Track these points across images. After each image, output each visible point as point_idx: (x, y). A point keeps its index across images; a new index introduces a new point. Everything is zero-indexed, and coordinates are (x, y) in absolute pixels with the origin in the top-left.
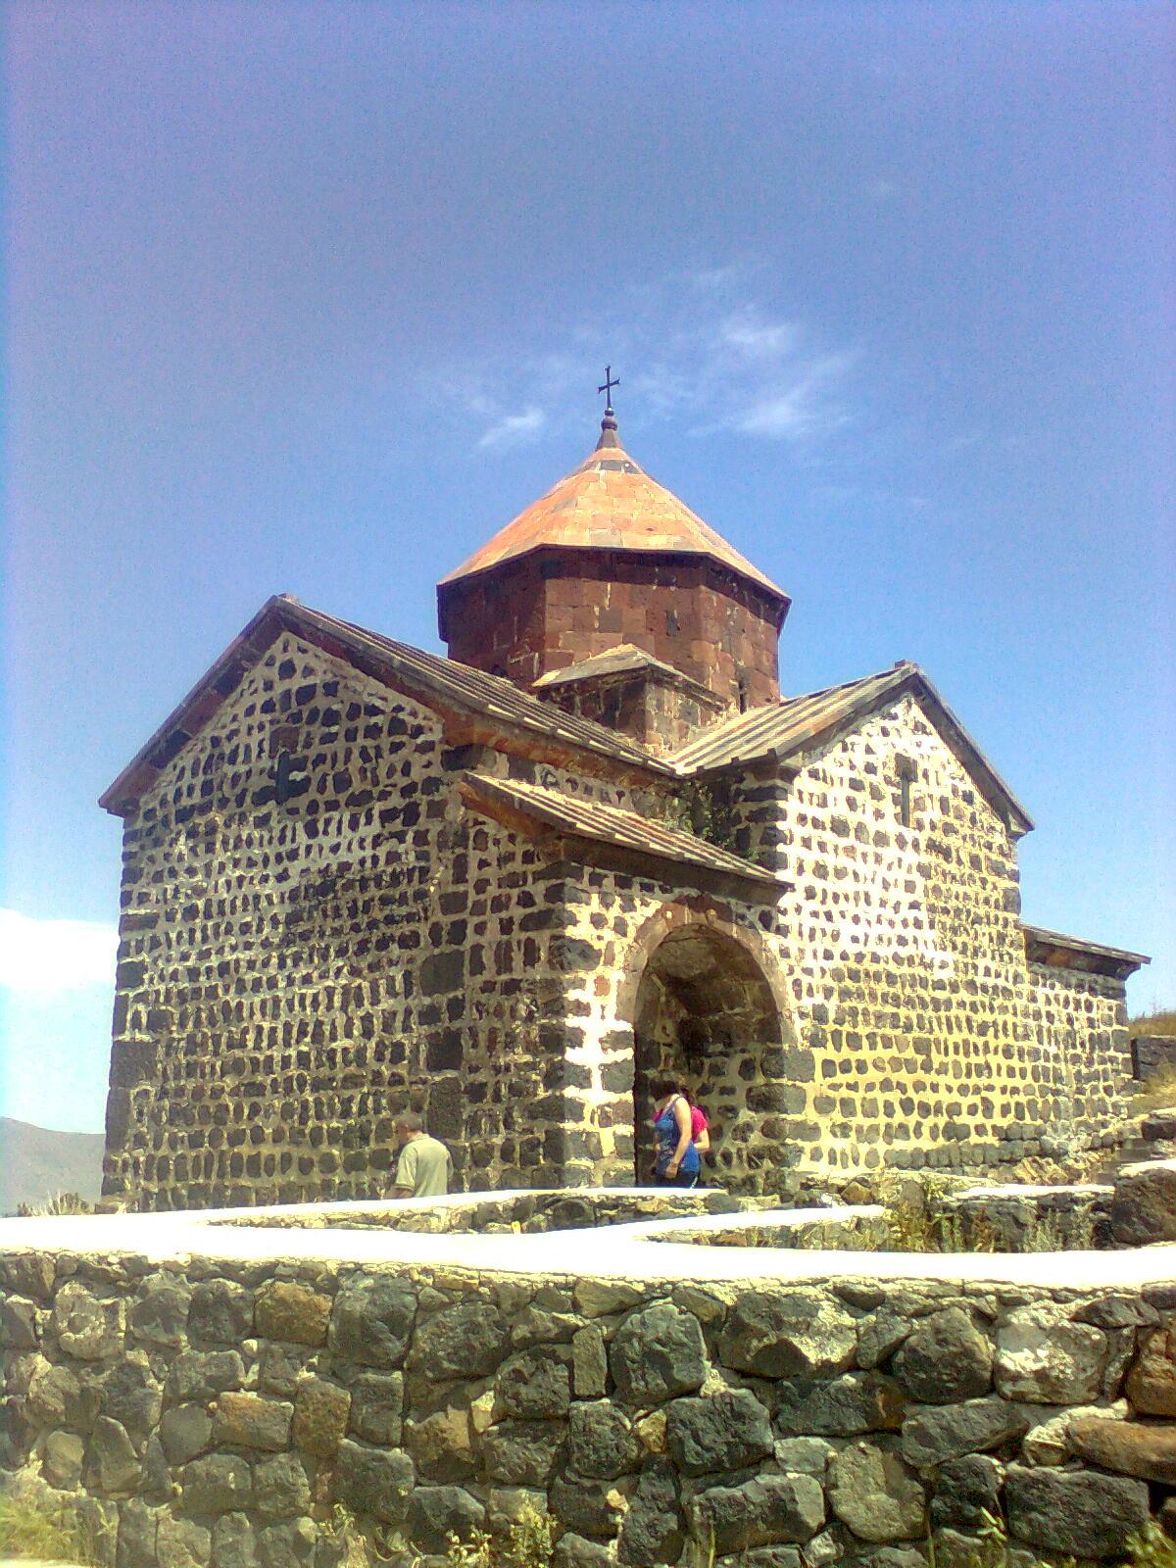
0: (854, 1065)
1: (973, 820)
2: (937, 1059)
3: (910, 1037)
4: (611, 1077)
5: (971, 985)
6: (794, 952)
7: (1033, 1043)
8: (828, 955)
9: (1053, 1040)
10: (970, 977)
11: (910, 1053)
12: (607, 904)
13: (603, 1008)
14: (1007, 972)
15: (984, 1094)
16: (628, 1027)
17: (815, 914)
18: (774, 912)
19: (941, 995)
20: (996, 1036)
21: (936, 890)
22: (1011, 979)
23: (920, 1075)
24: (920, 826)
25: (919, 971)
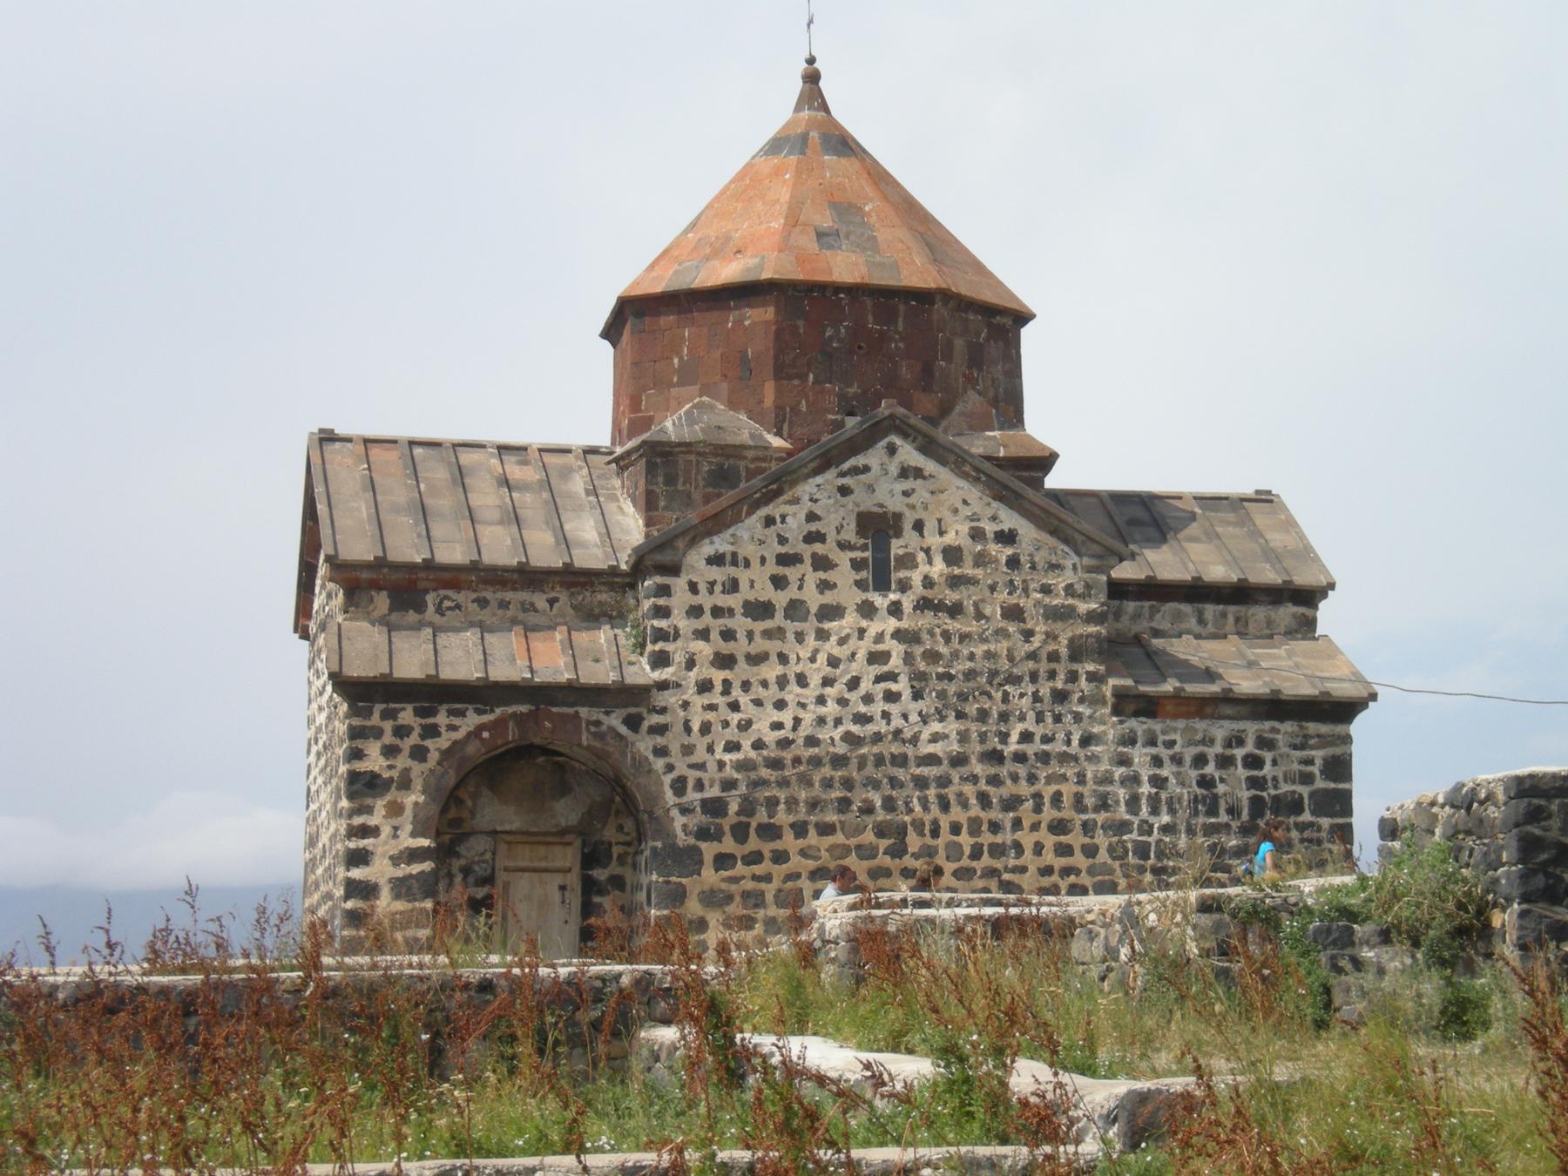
0: (767, 855)
1: (1013, 562)
2: (914, 842)
3: (869, 821)
4: (402, 887)
5: (995, 757)
6: (675, 749)
7: (1122, 813)
8: (732, 747)
9: (1164, 809)
10: (989, 746)
11: (869, 837)
12: (402, 731)
13: (396, 829)
14: (1069, 734)
15: (1006, 876)
16: (425, 842)
17: (712, 707)
18: (644, 711)
19: (930, 771)
20: (1038, 809)
21: (932, 656)
22: (1075, 742)
23: (887, 861)
24: (904, 587)
25: (896, 749)
